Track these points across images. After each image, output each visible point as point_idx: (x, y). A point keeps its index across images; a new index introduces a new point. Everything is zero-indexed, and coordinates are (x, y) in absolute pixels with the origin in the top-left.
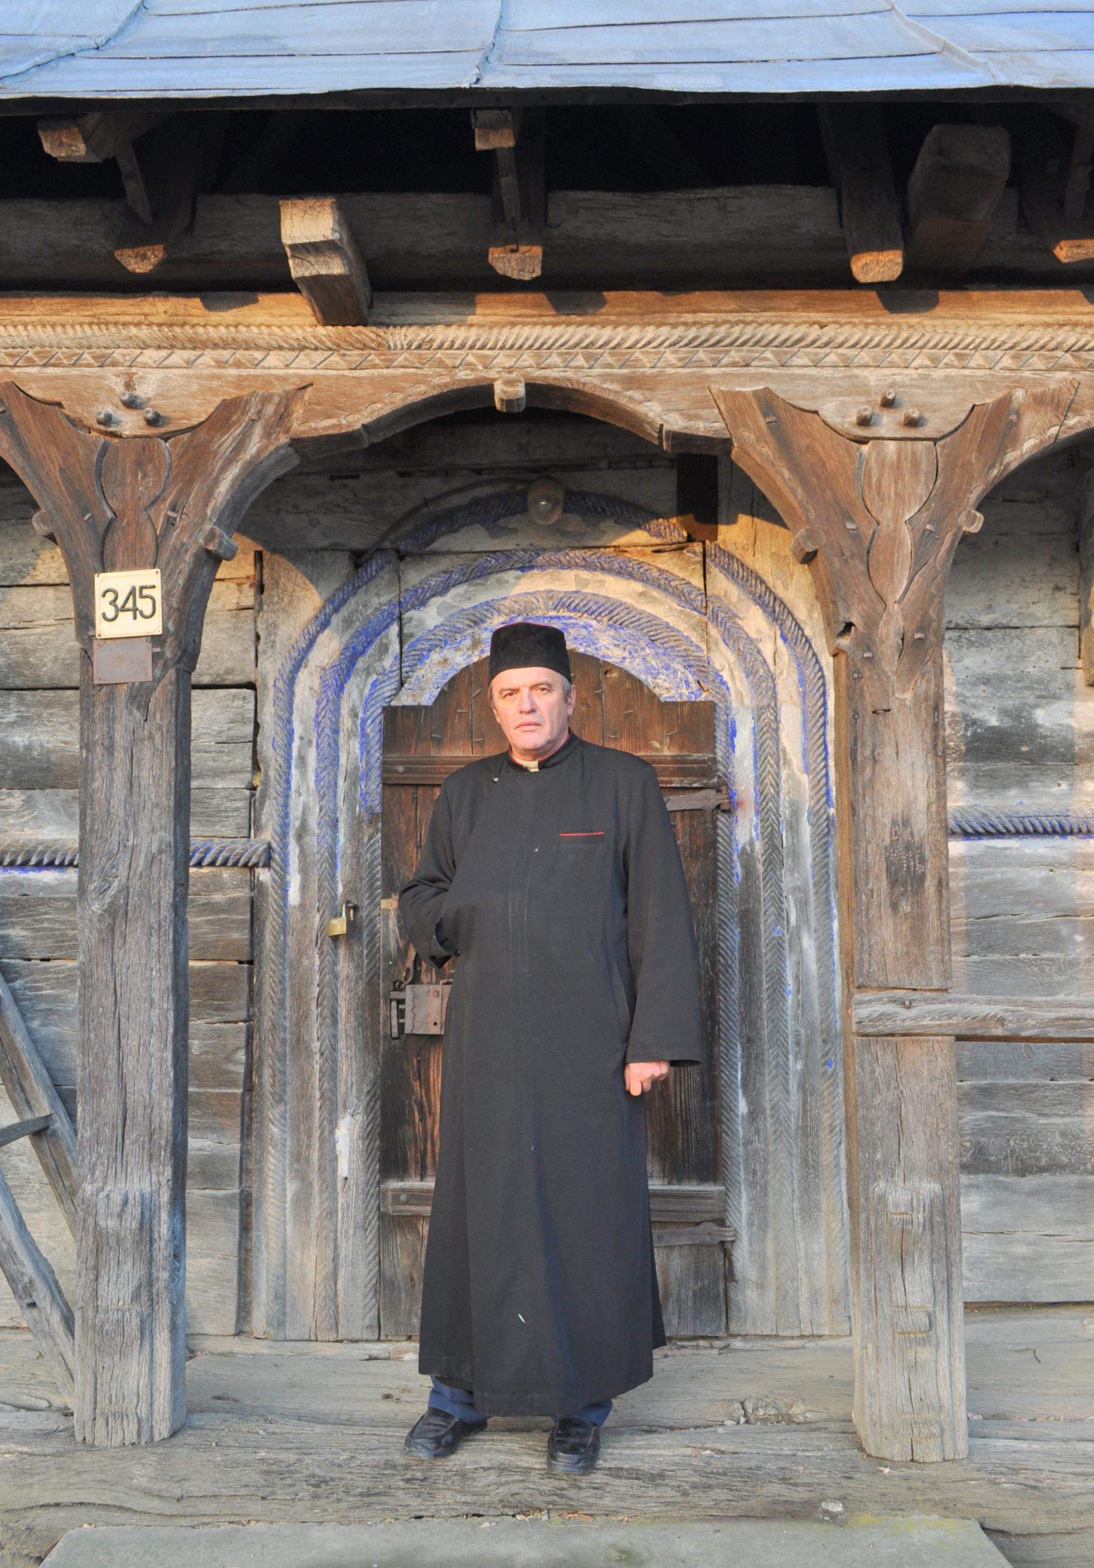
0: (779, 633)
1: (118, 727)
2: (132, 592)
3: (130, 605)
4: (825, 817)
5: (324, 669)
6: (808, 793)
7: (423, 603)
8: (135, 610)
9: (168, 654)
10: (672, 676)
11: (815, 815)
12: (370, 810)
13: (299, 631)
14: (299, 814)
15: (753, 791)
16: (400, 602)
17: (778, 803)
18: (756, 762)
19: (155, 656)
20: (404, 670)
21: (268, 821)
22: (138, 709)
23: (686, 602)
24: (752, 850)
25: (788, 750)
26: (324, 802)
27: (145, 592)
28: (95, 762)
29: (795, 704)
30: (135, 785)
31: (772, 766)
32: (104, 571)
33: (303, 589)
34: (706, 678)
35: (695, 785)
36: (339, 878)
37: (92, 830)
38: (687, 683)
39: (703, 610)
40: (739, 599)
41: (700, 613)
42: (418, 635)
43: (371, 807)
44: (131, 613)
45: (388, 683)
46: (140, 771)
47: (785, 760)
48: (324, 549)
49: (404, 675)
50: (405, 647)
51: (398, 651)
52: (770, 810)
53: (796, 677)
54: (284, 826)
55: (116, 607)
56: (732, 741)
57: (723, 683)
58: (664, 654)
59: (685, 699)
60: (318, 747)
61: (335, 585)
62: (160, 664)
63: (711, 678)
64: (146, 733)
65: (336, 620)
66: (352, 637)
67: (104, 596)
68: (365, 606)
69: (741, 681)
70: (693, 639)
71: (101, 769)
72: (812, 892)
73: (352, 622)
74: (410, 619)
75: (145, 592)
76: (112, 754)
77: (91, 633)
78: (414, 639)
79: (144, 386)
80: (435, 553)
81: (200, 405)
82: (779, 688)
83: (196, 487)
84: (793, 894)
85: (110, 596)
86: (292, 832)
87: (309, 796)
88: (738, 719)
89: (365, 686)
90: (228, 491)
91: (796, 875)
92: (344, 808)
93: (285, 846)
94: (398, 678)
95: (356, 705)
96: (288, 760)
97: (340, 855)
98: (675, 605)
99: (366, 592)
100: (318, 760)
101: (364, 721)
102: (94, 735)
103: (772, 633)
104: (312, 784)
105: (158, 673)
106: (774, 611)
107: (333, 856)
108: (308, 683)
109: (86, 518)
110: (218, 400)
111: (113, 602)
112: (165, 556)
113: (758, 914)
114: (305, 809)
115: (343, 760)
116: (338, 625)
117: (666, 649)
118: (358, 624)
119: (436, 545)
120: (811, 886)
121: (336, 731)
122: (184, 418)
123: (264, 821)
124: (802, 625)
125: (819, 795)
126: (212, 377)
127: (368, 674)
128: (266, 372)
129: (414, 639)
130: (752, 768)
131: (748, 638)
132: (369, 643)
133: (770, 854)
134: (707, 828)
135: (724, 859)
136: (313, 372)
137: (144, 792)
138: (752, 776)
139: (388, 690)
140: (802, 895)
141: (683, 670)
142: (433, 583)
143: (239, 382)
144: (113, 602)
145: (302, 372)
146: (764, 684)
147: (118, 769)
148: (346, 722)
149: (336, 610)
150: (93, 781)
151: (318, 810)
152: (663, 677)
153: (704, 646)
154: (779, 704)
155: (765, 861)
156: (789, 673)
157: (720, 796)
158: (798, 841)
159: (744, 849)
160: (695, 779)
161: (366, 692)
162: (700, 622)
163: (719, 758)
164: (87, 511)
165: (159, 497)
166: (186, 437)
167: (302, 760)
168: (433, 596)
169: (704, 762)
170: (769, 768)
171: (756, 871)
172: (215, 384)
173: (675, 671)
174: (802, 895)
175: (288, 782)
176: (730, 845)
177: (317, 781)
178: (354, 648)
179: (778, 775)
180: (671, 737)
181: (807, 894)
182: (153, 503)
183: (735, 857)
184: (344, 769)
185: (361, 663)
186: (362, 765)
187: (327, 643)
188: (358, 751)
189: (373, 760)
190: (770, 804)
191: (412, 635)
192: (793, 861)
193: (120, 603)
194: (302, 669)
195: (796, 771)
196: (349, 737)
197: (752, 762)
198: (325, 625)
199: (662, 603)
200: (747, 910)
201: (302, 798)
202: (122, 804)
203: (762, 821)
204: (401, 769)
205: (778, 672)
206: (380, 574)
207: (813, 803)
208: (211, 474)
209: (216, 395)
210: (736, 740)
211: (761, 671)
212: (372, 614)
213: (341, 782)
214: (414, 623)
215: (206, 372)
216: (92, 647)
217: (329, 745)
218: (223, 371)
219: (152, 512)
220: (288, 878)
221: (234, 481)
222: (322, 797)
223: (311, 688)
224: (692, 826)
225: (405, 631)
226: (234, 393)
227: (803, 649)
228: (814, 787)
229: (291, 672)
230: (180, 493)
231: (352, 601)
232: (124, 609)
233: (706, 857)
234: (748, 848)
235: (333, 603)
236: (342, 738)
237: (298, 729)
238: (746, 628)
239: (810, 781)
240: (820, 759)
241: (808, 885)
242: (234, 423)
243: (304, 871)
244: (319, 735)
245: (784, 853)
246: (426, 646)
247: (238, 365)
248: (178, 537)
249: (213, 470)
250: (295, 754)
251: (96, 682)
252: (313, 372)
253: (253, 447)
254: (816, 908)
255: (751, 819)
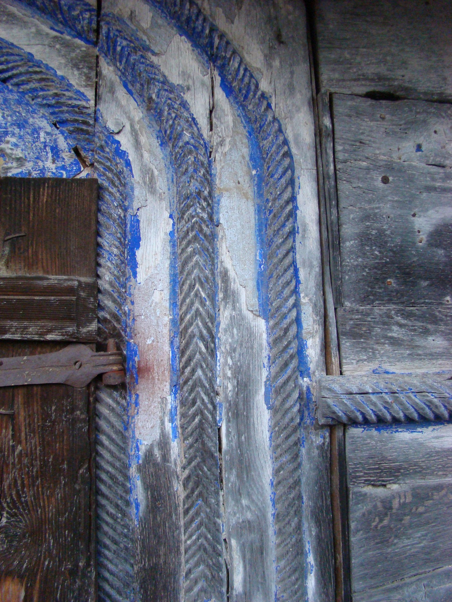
0: (218, 80)
4: (296, 395)
6: (265, 353)
10: (29, 138)
11: (278, 392)
15: (167, 348)
17: (212, 370)
18: (173, 294)
23: (65, 23)
24: (165, 457)
25: (232, 274)
29: (245, 195)
31: (203, 303)
34: (90, 142)
35: (50, 337)
38: (56, 151)
39: (92, 36)
40: (154, 24)
41: (87, 41)
47: (226, 290)
52: (198, 383)
53: (245, 151)
56: (133, 255)
57: (122, 154)
58: (19, 102)
59: (48, 175)
63: (98, 142)
69: (150, 151)
70: (72, 82)
72: (271, 530)
82: (217, 167)
84: (239, 536)
88: (143, 216)
91: (245, 502)
98: (46, 29)
103: (207, 79)
106: (211, 44)
113: (174, 574)
117: (24, 93)
120: (270, 518)
124: (255, 74)
125: (286, 356)
130: (167, 304)
131: (165, 82)
133: (198, 466)
134: (74, 421)
135: (112, 477)
138: (167, 319)
140: (253, 536)
141: (49, 129)
146: (191, 158)
152: (14, 140)
153: (90, 94)
154: (216, 194)
155: (188, 478)
156: (234, 145)
157: (102, 358)
158: (248, 438)
159: (149, 453)
160: (50, 324)
162: (85, 57)
163: (104, 284)
169: (71, 291)
170: (197, 305)
171: (172, 496)
173: (36, 131)
174: (253, 536)
176: (123, 450)
179: (213, 318)
180: (14, 243)
181: (262, 532)
183: (133, 471)
190: (199, 372)
192: (239, 476)
195: (245, 312)
197: (166, 294)
199: (24, 24)
200: (154, 568)
203: (183, 404)
205: (215, 140)
207: (274, 370)
210: (139, 253)
211: (187, 136)
224: (46, 416)
227: (258, 105)
228: (276, 341)
233: (73, 478)
234: (157, 453)
238: (162, 69)
239: (271, 330)
240: (287, 292)
241: (264, 516)
245: (226, 457)
254: (278, 559)
255: (163, 400)
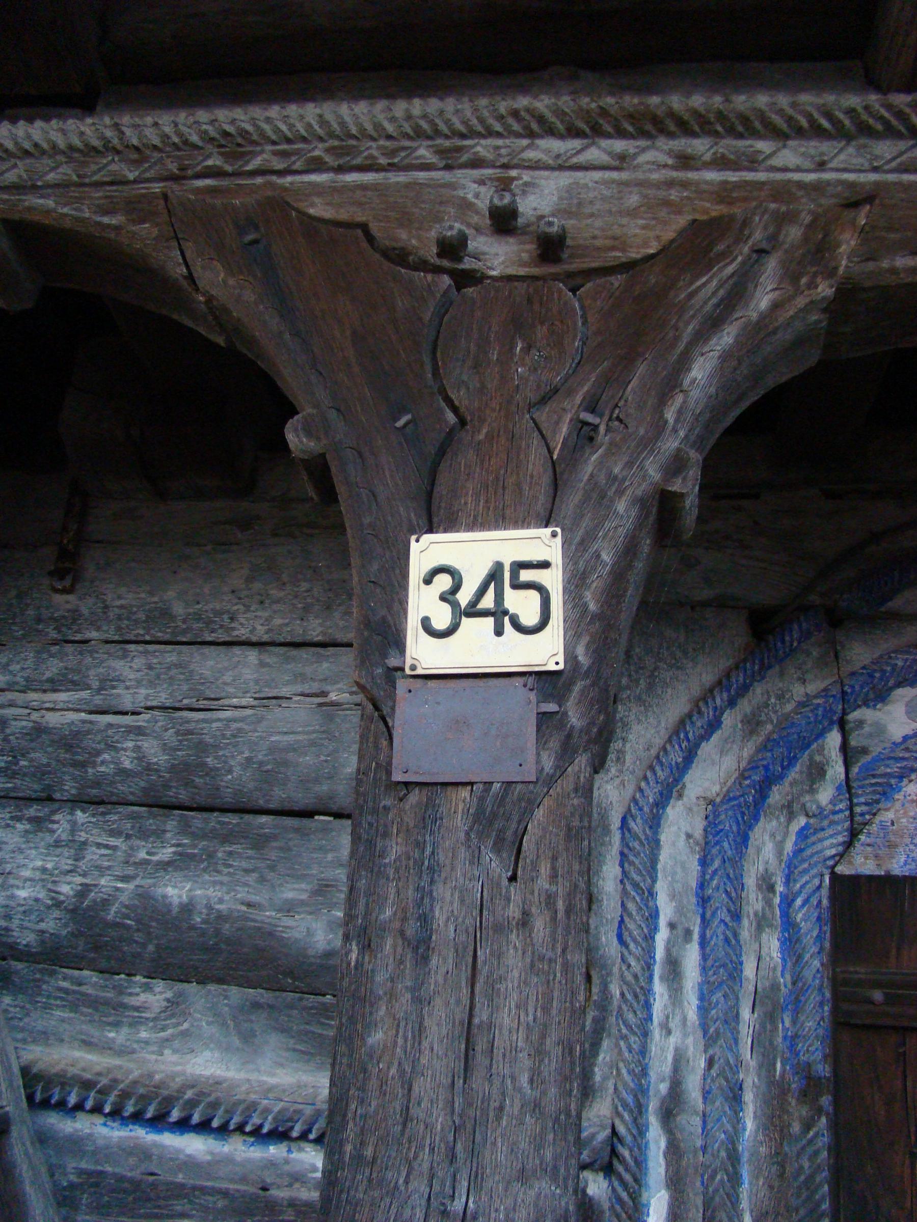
1: (442, 891)
2: (495, 576)
3: (488, 602)
5: (711, 802)
7: (881, 697)
8: (499, 613)
9: (575, 719)
12: (805, 1072)
13: (664, 734)
14: (667, 1068)
16: (844, 693)
19: (543, 718)
20: (858, 810)
21: (605, 1078)
22: (498, 847)
26: (715, 1050)
27: (526, 575)
28: (380, 978)
30: (481, 1045)
32: (430, 531)
33: (671, 666)
36: (744, 1204)
37: (358, 1158)
42: (875, 750)
43: (808, 1065)
44: (490, 621)
45: (830, 831)
46: (494, 1010)
48: (705, 604)
49: (858, 819)
50: (855, 770)
51: (843, 776)
54: (641, 1092)
55: (455, 605)
60: (703, 944)
61: (725, 663)
62: (554, 743)
64: (514, 911)
65: (729, 719)
66: (758, 751)
67: (428, 581)
68: (780, 697)
71: (392, 995)
73: (759, 723)
74: (860, 723)
75: (526, 575)
76: (425, 959)
77: (393, 662)
78: (868, 758)
79: (531, 198)
80: (896, 616)
81: (644, 228)
83: (642, 369)
85: (444, 582)
86: (653, 1105)
87: (685, 1035)
89: (786, 834)
90: (711, 376)
92: (753, 1064)
93: (641, 1130)
94: (847, 824)
95: (771, 869)
96: (648, 967)
97: (745, 1158)
99: (782, 674)
100: (704, 969)
101: (788, 901)
102: (381, 909)
104: (692, 1015)
105: (548, 764)
107: (734, 1157)
108: (685, 827)
109: (400, 424)
110: (682, 221)
111: (448, 597)
112: (571, 500)
114: (679, 1060)
115: (749, 971)
116: (734, 727)
118: (769, 727)
119: (896, 603)
121: (736, 916)
122: (613, 248)
123: (598, 1078)
126: (670, 184)
127: (791, 816)
128: (779, 176)
129: (868, 758)
132: (792, 761)
136: (873, 177)
137: (501, 1067)
139: (830, 844)
142: (900, 663)
143: (724, 193)
144: (448, 597)
145: (850, 177)
147: (438, 1002)
148: (753, 902)
149: (732, 703)
150: (370, 1026)
151: (702, 1064)
161: (789, 846)
164: (403, 410)
165: (556, 391)
166: (617, 281)
167: (674, 967)
168: (899, 685)
172: (674, 195)
175: (648, 1006)
177: (704, 1010)
178: (766, 768)
182: (544, 400)
184: (751, 988)
185: (776, 796)
186: (784, 981)
187: (716, 758)
188: (776, 954)
189: (808, 974)
191: (864, 751)
193: (464, 597)
194: (672, 801)
196: (759, 928)
198: (714, 725)
201: (673, 1040)
202: (443, 1095)
204: (878, 995)
206: (804, 646)
208: (673, 346)
209: (679, 212)
212: (796, 711)
213: (746, 1013)
214: (867, 729)
215: (655, 176)
216: (392, 696)
217: (727, 940)
218: (691, 175)
219: (542, 416)
220: (645, 1195)
221: (725, 357)
222: (710, 1040)
223: (689, 836)
225: (853, 743)
226: (716, 210)
229: (657, 804)
230: (606, 380)
231: (758, 691)
232: (473, 611)
235: (729, 691)
236: (746, 931)
237: (666, 910)
242: (723, 255)
243: (675, 1183)
244: (705, 923)
246: (894, 768)
247: (721, 163)
248: (600, 463)
249: (677, 338)
250: (660, 953)
251: (397, 777)
252: (873, 177)
253: (763, 301)
